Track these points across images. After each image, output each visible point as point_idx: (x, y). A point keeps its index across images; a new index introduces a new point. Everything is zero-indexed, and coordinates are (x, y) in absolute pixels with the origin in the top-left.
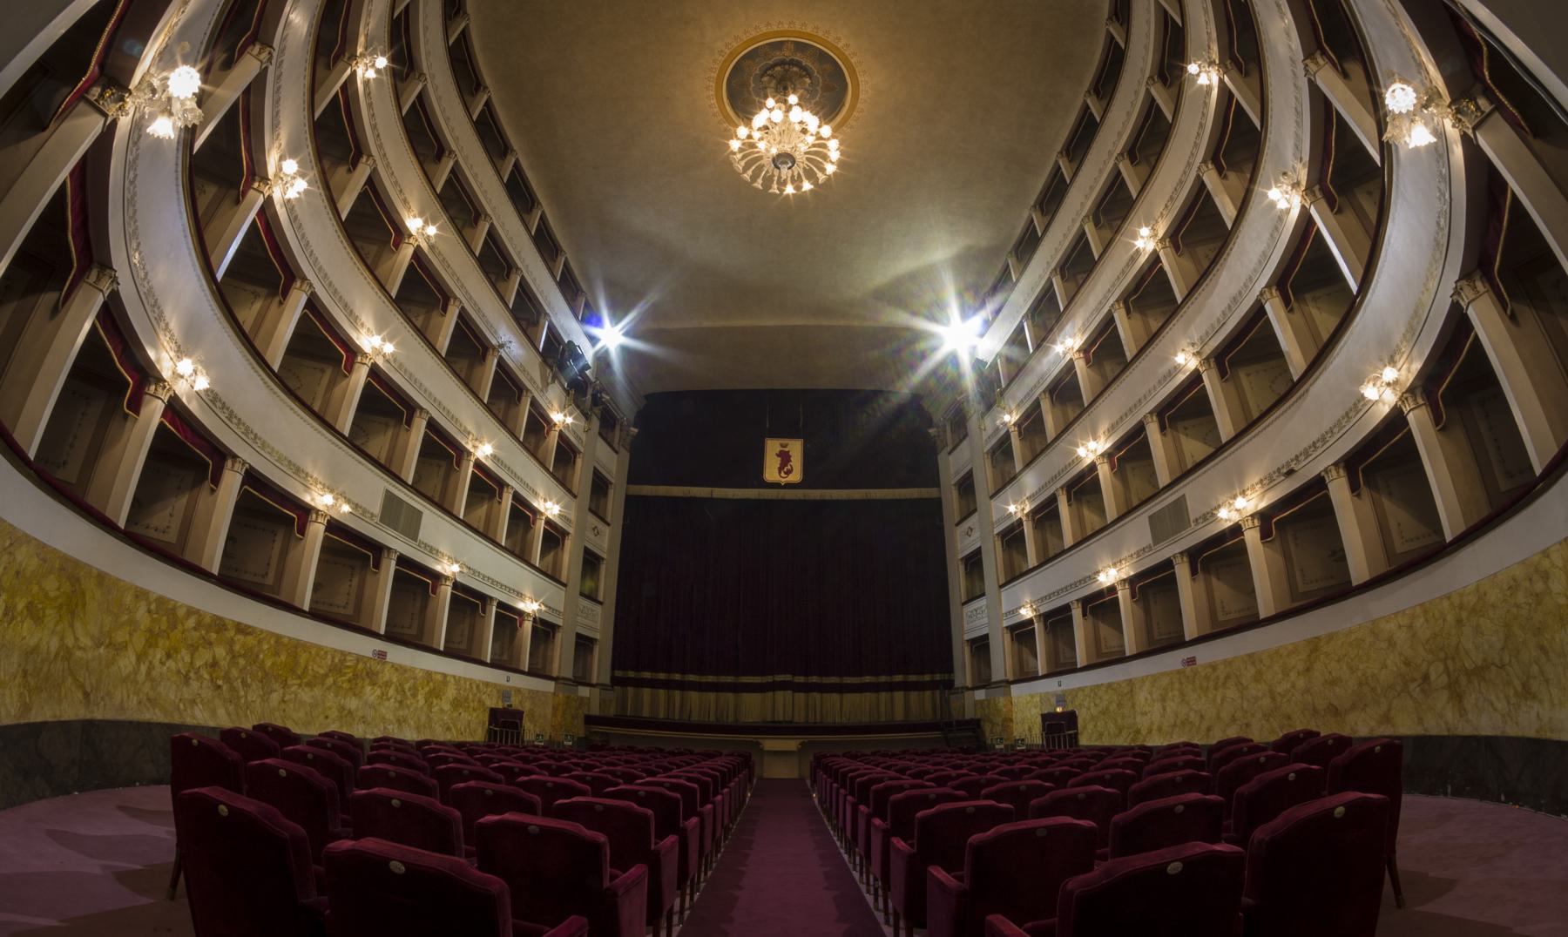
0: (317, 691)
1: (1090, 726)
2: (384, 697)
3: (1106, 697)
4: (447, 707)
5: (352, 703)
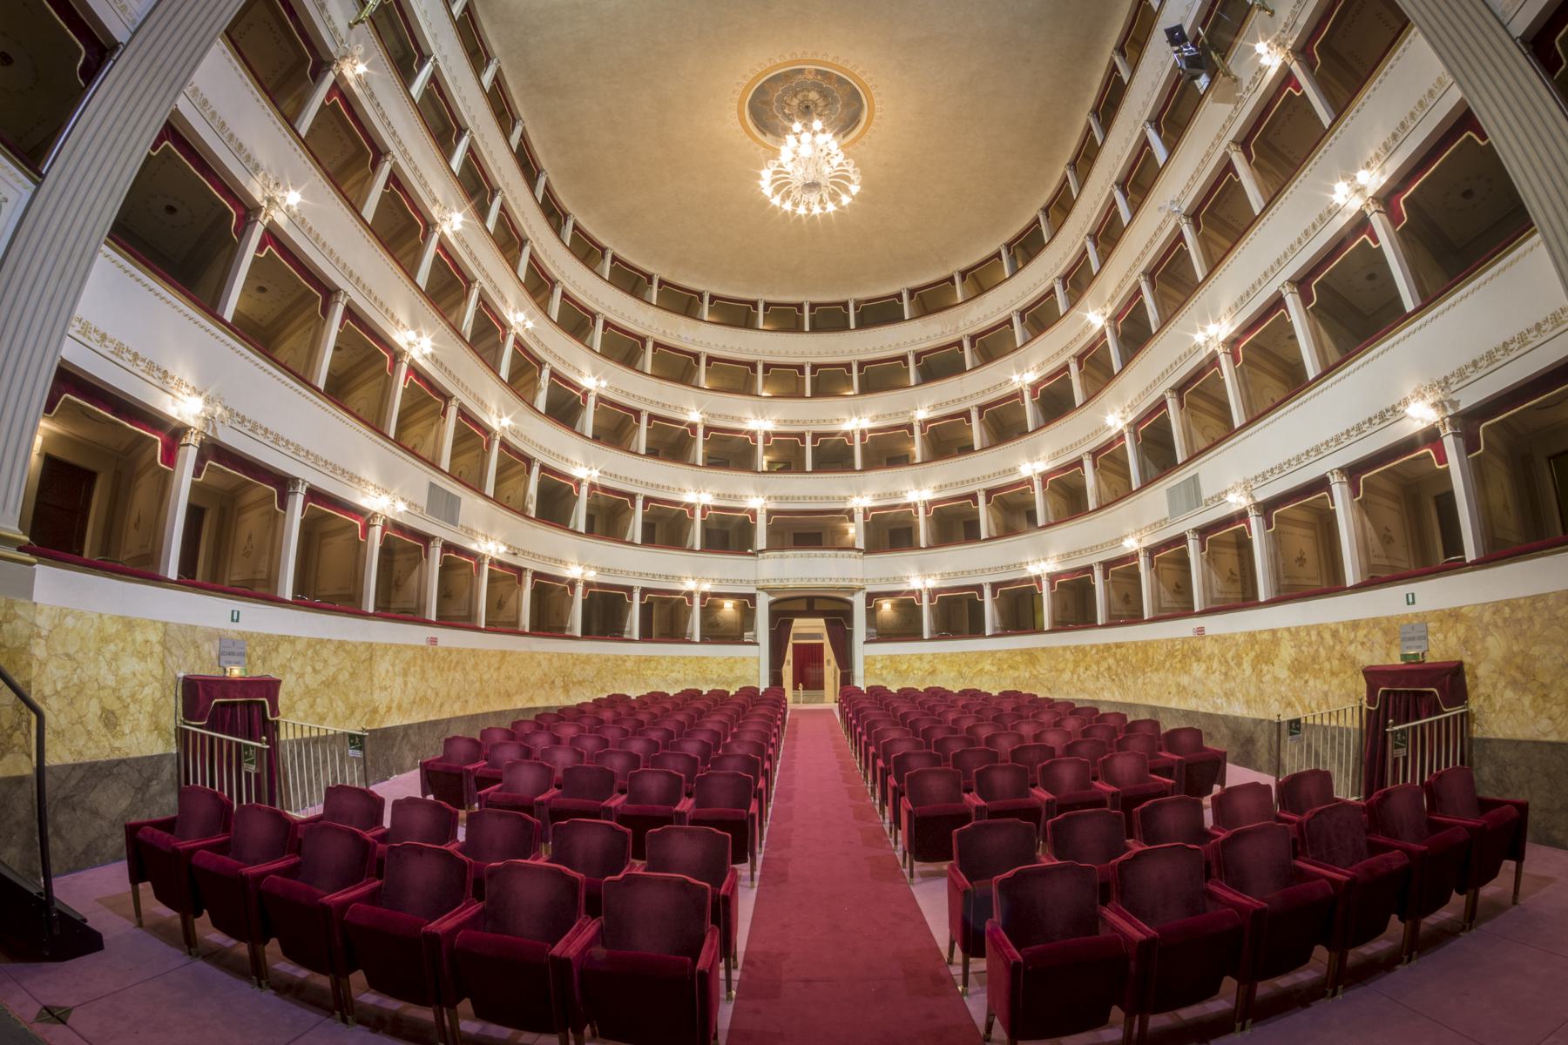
0: (1162, 674)
1: (302, 706)
2: (1209, 671)
3: (333, 661)
4: (1284, 674)
5: (1185, 680)
